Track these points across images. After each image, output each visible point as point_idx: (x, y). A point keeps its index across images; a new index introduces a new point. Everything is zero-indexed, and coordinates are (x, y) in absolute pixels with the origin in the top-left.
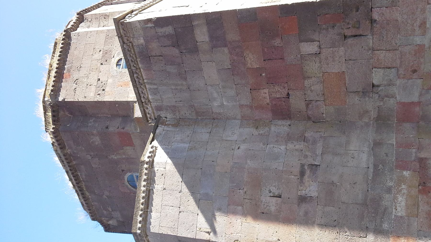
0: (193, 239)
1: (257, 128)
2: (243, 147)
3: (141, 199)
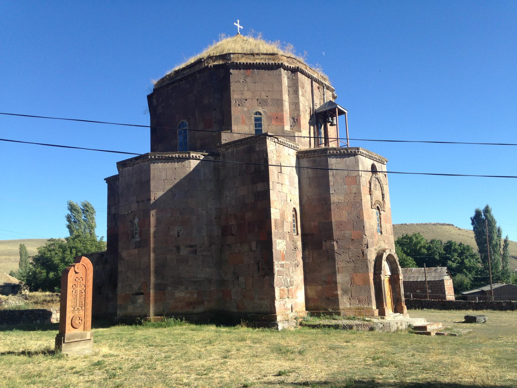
1: (216, 218)
2: (204, 212)
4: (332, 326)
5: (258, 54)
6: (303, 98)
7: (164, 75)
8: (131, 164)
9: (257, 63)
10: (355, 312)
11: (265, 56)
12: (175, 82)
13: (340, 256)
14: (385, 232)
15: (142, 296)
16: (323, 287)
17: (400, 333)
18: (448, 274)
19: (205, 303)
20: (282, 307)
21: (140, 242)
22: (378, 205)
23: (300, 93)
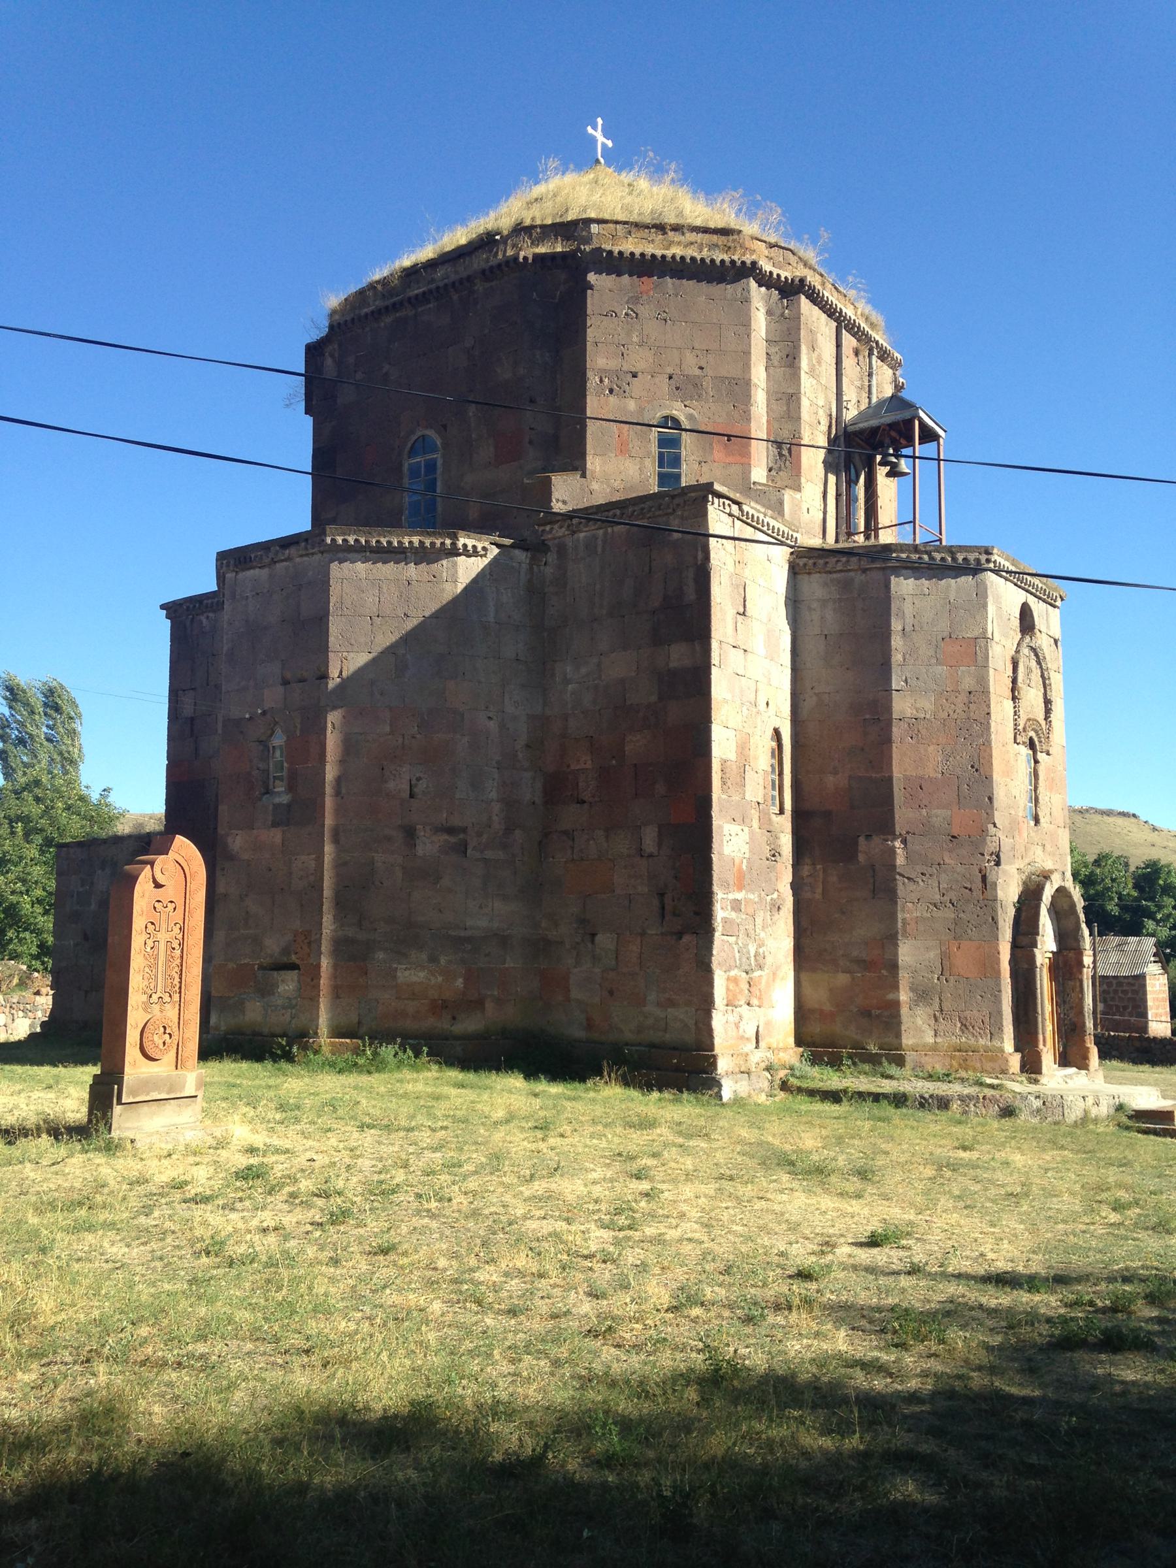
0: (328, 647)
1: (528, 746)
2: (493, 726)
3: (387, 539)
4: (885, 1096)
5: (677, 228)
6: (811, 379)
7: (364, 283)
8: (266, 561)
9: (673, 257)
10: (952, 1057)
11: (700, 235)
12: (401, 303)
13: (912, 886)
14: (1048, 818)
15: (294, 974)
16: (853, 979)
17: (1091, 1127)
18: (1157, 959)
19: (489, 1005)
20: (733, 1032)
21: (289, 806)
22: (1032, 734)
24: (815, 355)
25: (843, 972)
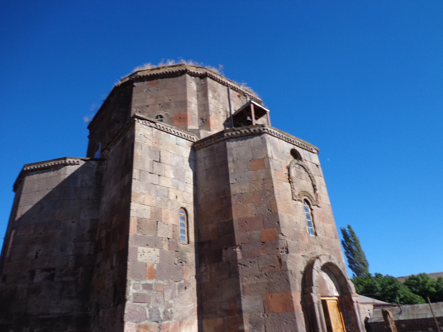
1: (89, 232)
2: (74, 225)
6: (214, 100)
13: (246, 269)
23: (210, 95)
24: (216, 95)
25: (220, 317)
